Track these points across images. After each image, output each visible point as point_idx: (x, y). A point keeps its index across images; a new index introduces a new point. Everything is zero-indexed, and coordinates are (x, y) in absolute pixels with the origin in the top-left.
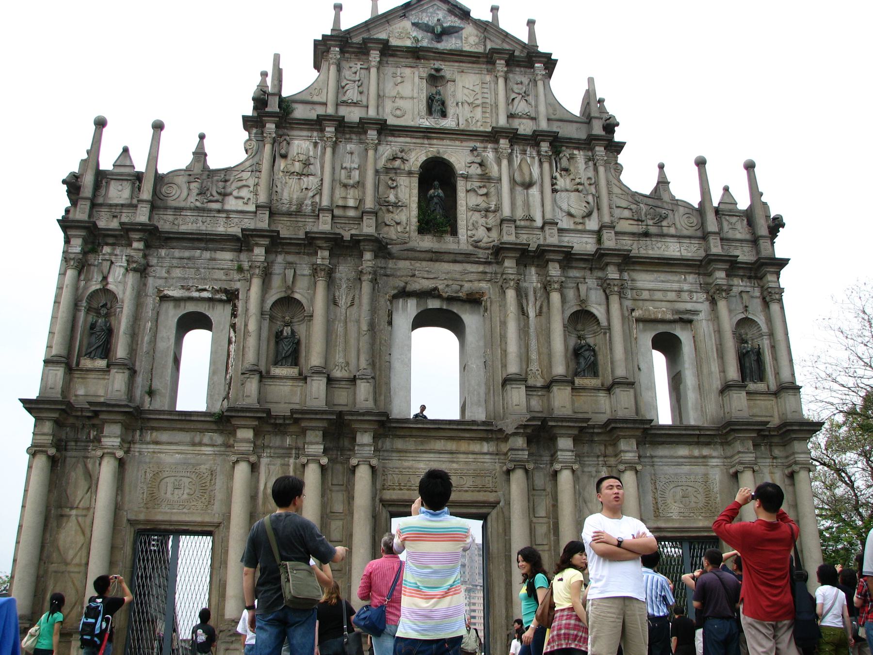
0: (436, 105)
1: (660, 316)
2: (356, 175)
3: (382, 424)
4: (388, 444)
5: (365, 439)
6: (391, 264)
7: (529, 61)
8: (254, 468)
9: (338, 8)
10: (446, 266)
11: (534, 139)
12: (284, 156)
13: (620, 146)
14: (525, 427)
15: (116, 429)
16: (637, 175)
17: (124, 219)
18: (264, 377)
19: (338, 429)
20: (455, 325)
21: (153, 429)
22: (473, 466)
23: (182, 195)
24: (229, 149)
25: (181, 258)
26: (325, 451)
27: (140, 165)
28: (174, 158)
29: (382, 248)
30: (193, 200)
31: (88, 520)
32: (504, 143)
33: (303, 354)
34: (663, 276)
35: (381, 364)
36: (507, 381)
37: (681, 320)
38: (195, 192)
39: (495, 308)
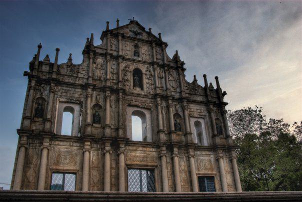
0: (136, 53)
1: (196, 116)
3: (127, 142)
8: (90, 152)
9: (108, 23)
10: (141, 99)
12: (95, 63)
13: (185, 70)
14: (165, 144)
15: (48, 140)
16: (189, 79)
17: (48, 76)
18: (92, 126)
20: (142, 115)
21: (57, 140)
22: (151, 155)
23: (64, 71)
25: (66, 90)
27: (52, 60)
28: (63, 60)
29: (124, 92)
31: (37, 168)
33: (102, 120)
34: (197, 106)
35: (122, 126)
36: (159, 132)
37: (201, 118)
38: (69, 70)
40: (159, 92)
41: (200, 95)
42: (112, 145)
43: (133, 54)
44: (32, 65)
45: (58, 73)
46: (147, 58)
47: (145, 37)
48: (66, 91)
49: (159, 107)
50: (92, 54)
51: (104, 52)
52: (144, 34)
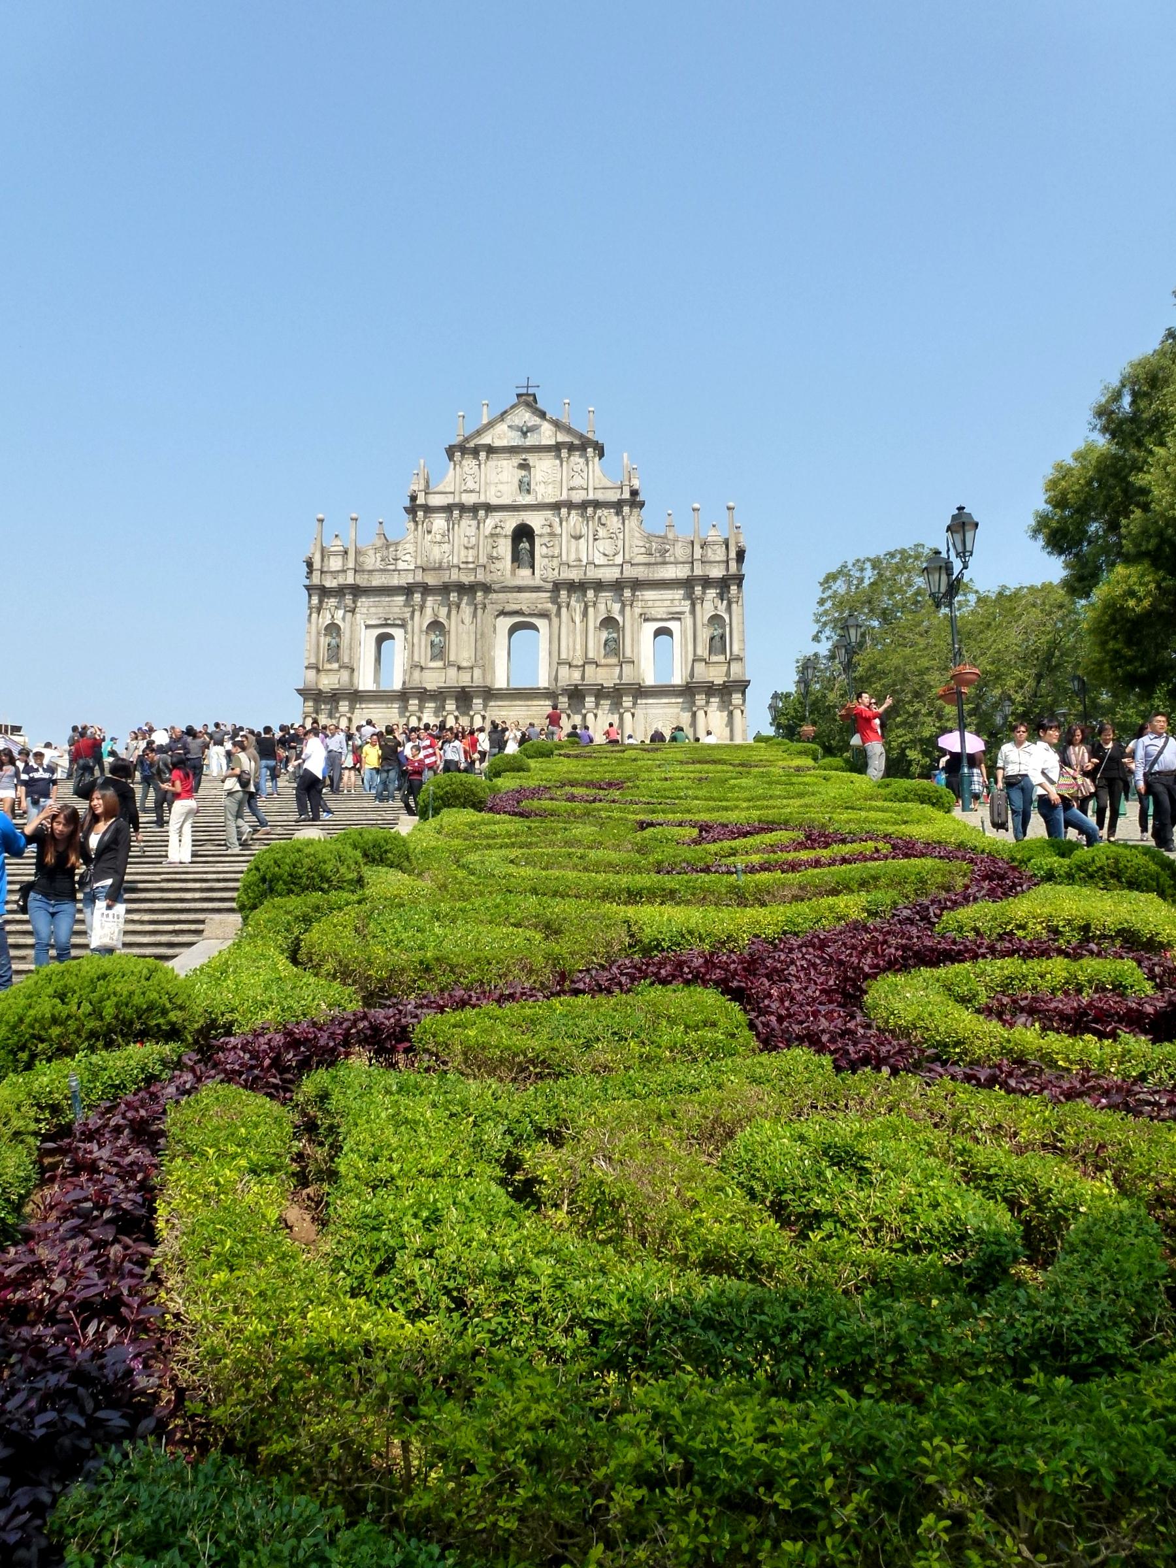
0: (525, 487)
2: (473, 540)
6: (493, 596)
10: (527, 595)
11: (583, 506)
12: (429, 532)
13: (642, 505)
17: (341, 580)
19: (464, 697)
23: (372, 561)
26: (457, 708)
29: (487, 588)
30: (379, 565)
32: (564, 511)
39: (555, 620)
41: (676, 563)
42: (457, 700)
43: (516, 483)
46: (545, 492)
50: (420, 514)
51: (449, 500)
52: (546, 427)
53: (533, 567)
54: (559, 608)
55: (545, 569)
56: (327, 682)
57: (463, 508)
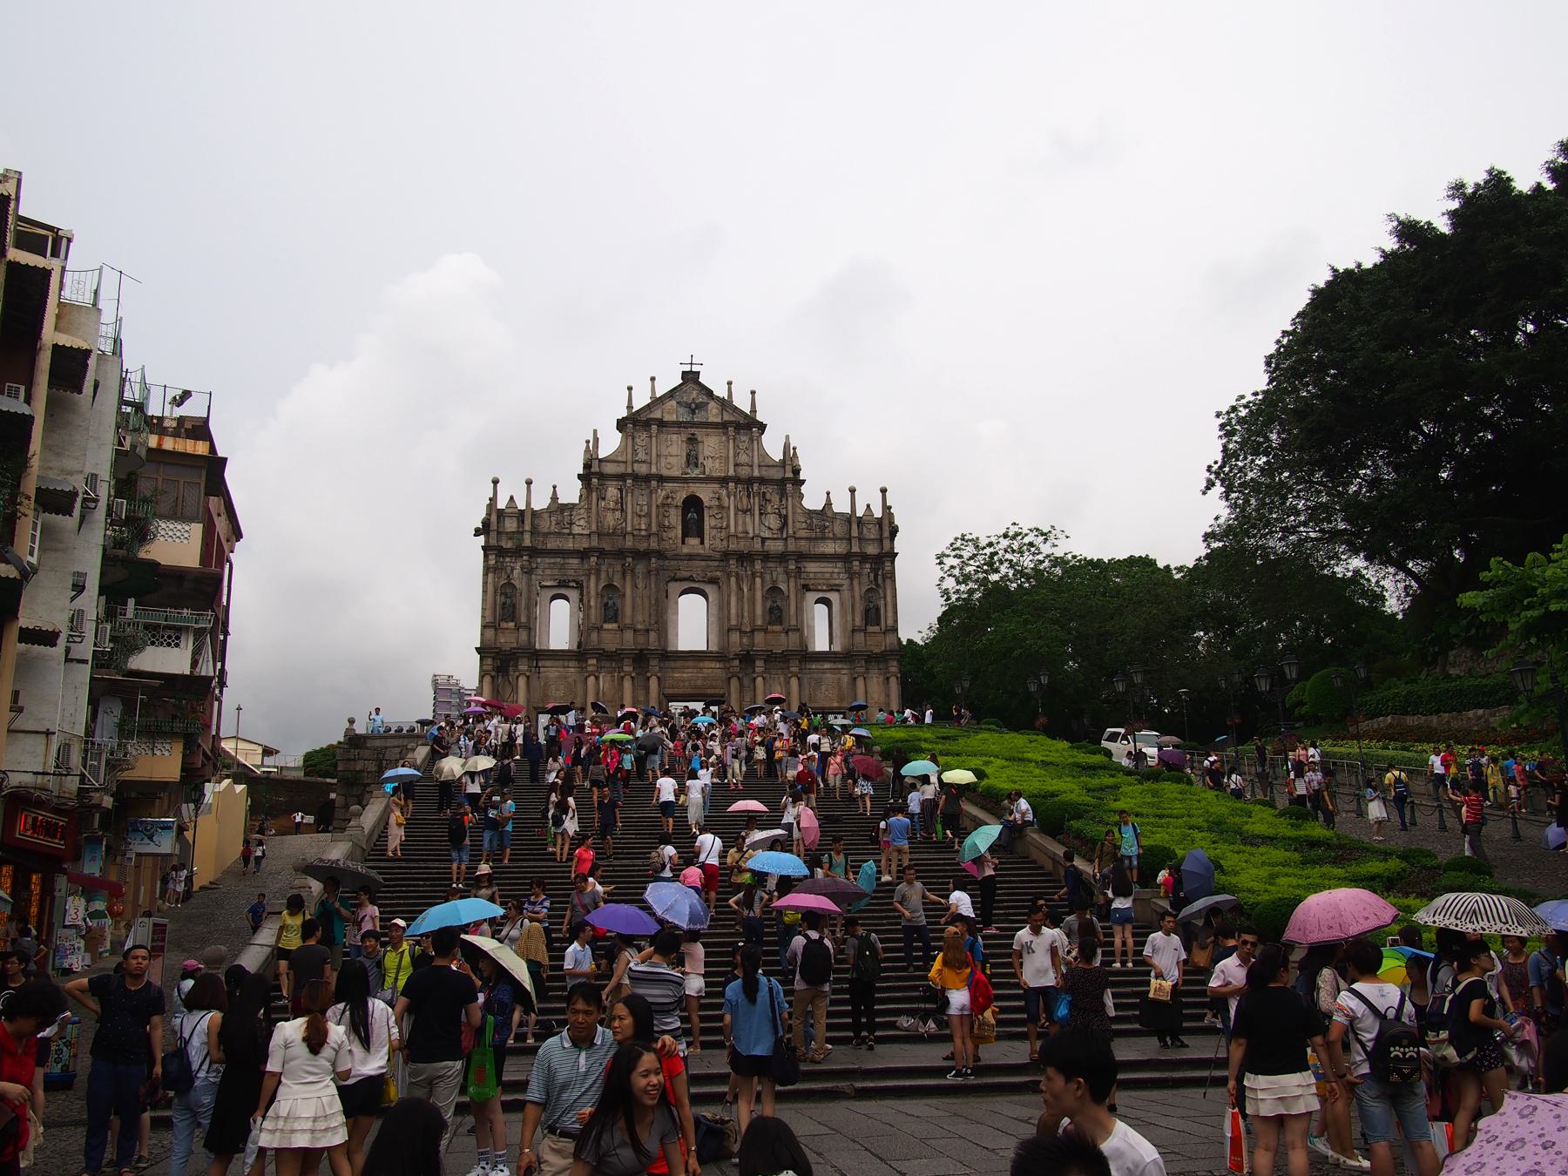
0: (692, 460)
4: (667, 664)
5: (653, 662)
7: (750, 426)
8: (597, 678)
11: (750, 481)
16: (812, 499)
19: (641, 659)
23: (545, 525)
24: (571, 493)
27: (521, 506)
28: (540, 502)
29: (660, 555)
30: (554, 528)
32: (731, 485)
39: (724, 587)
40: (733, 547)
41: (835, 538)
44: (486, 523)
45: (534, 531)
46: (713, 467)
47: (713, 414)
48: (552, 566)
49: (733, 580)
50: (595, 481)
51: (620, 469)
52: (713, 407)
53: (701, 535)
54: (729, 576)
55: (712, 540)
56: (507, 640)
57: (636, 477)
